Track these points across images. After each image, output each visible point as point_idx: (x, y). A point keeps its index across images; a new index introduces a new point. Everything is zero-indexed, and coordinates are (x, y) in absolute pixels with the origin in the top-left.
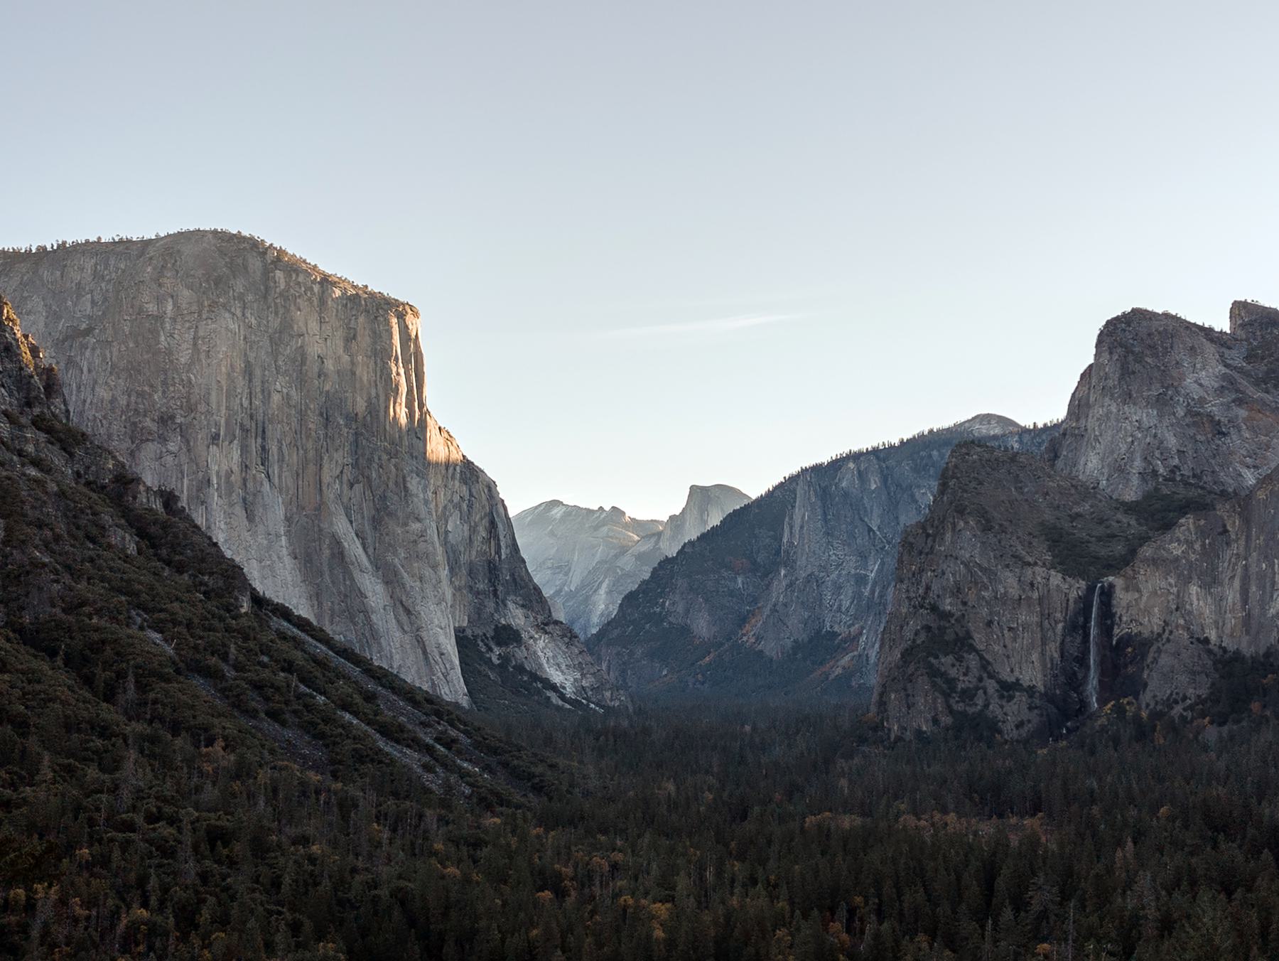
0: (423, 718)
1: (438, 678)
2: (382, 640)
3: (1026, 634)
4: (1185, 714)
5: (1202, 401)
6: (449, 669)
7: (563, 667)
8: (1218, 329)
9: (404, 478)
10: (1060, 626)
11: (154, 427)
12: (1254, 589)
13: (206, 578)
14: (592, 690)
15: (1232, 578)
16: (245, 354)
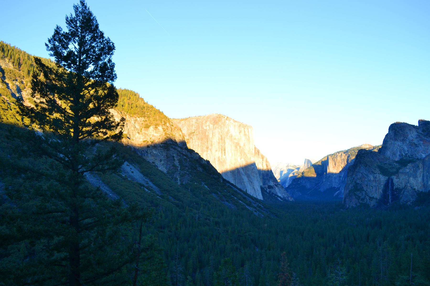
0: (254, 202)
2: (247, 188)
5: (412, 140)
7: (281, 193)
8: (416, 125)
10: (382, 186)
11: (206, 149)
12: (425, 178)
13: (215, 176)
15: (420, 176)
16: (221, 136)
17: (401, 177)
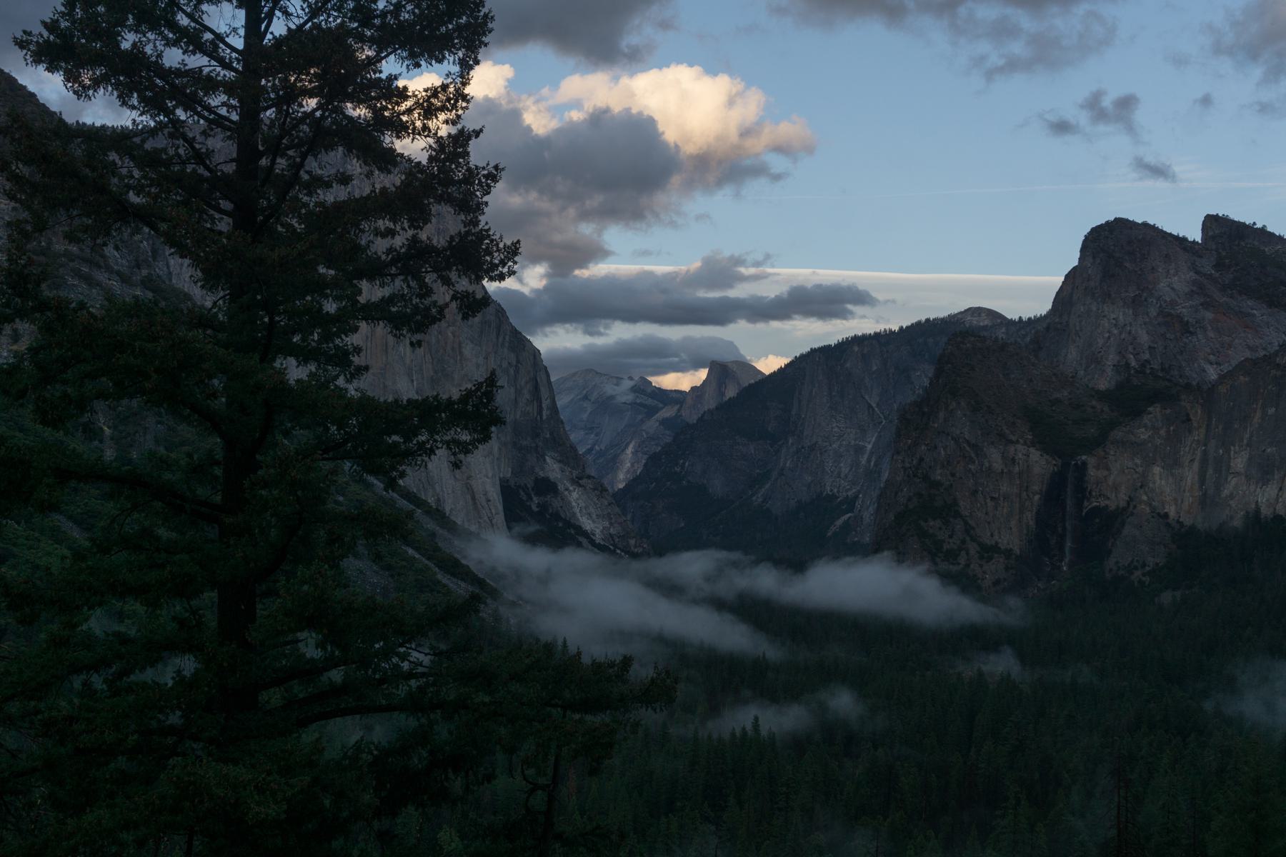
1: (485, 521)
3: (1006, 504)
4: (1144, 579)
6: (494, 514)
7: (594, 516)
8: (1190, 239)
9: (460, 344)
10: (1037, 497)
12: (1210, 471)
14: (619, 538)
15: (1192, 461)
17: (1116, 461)
